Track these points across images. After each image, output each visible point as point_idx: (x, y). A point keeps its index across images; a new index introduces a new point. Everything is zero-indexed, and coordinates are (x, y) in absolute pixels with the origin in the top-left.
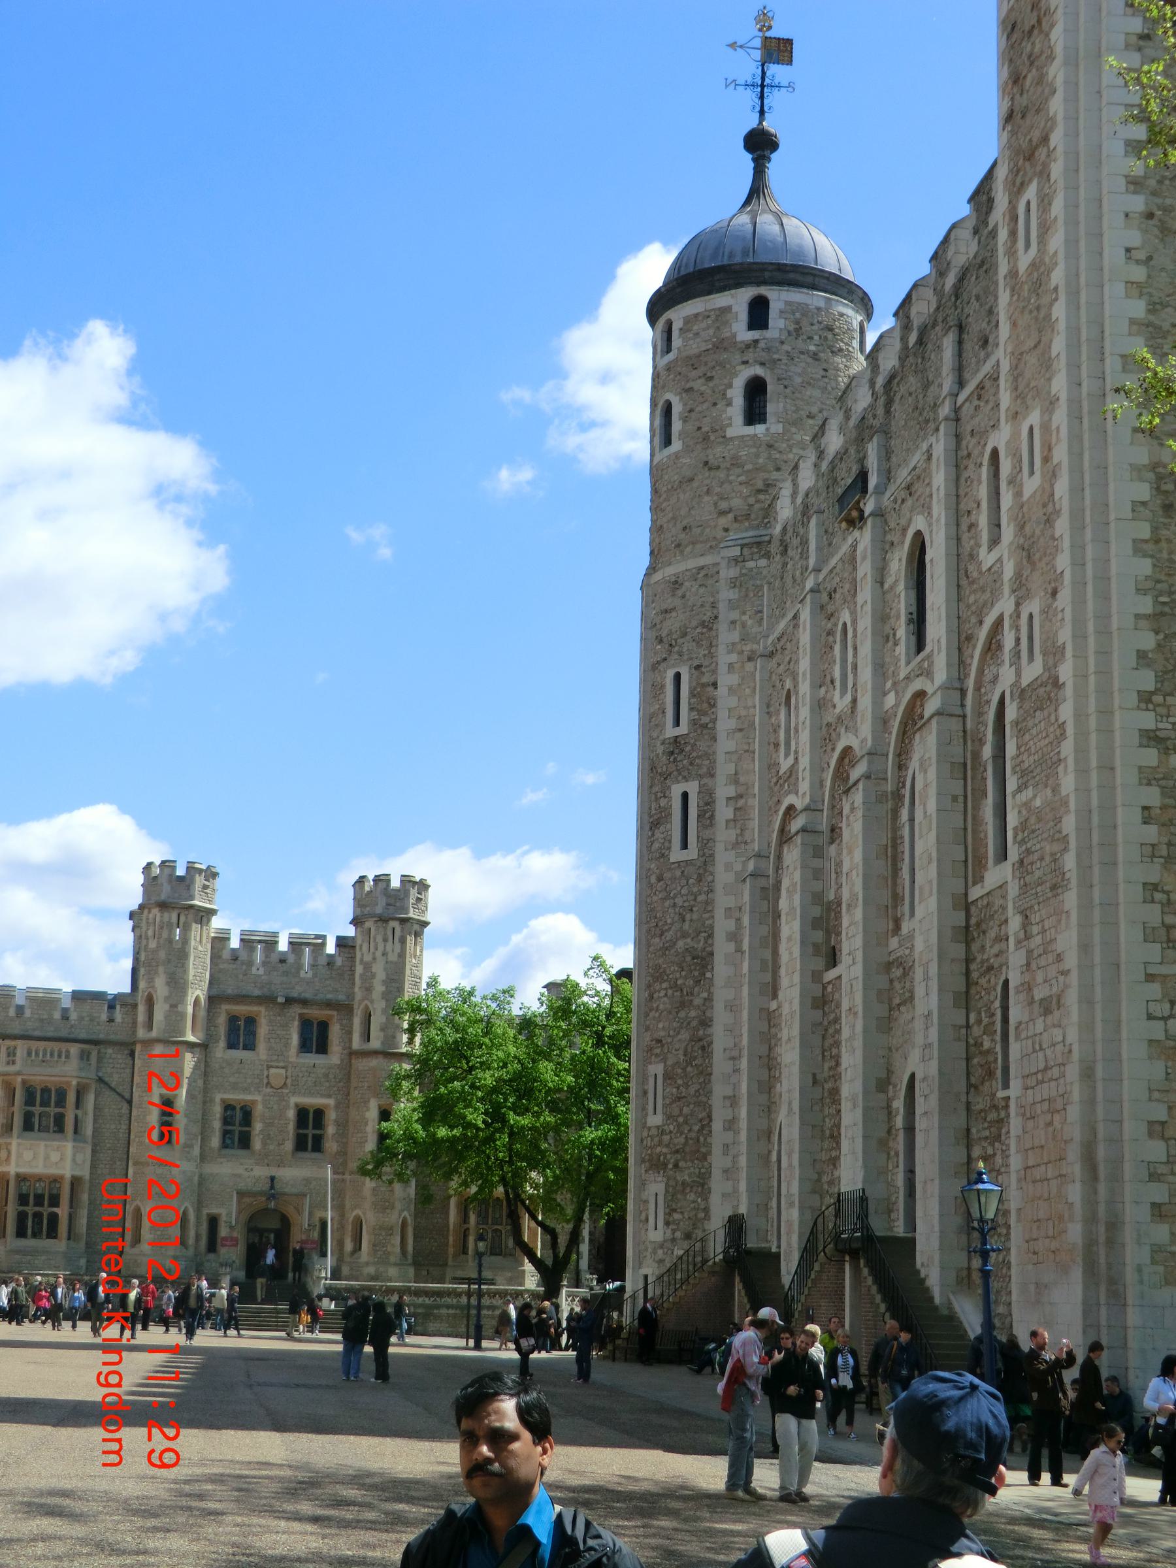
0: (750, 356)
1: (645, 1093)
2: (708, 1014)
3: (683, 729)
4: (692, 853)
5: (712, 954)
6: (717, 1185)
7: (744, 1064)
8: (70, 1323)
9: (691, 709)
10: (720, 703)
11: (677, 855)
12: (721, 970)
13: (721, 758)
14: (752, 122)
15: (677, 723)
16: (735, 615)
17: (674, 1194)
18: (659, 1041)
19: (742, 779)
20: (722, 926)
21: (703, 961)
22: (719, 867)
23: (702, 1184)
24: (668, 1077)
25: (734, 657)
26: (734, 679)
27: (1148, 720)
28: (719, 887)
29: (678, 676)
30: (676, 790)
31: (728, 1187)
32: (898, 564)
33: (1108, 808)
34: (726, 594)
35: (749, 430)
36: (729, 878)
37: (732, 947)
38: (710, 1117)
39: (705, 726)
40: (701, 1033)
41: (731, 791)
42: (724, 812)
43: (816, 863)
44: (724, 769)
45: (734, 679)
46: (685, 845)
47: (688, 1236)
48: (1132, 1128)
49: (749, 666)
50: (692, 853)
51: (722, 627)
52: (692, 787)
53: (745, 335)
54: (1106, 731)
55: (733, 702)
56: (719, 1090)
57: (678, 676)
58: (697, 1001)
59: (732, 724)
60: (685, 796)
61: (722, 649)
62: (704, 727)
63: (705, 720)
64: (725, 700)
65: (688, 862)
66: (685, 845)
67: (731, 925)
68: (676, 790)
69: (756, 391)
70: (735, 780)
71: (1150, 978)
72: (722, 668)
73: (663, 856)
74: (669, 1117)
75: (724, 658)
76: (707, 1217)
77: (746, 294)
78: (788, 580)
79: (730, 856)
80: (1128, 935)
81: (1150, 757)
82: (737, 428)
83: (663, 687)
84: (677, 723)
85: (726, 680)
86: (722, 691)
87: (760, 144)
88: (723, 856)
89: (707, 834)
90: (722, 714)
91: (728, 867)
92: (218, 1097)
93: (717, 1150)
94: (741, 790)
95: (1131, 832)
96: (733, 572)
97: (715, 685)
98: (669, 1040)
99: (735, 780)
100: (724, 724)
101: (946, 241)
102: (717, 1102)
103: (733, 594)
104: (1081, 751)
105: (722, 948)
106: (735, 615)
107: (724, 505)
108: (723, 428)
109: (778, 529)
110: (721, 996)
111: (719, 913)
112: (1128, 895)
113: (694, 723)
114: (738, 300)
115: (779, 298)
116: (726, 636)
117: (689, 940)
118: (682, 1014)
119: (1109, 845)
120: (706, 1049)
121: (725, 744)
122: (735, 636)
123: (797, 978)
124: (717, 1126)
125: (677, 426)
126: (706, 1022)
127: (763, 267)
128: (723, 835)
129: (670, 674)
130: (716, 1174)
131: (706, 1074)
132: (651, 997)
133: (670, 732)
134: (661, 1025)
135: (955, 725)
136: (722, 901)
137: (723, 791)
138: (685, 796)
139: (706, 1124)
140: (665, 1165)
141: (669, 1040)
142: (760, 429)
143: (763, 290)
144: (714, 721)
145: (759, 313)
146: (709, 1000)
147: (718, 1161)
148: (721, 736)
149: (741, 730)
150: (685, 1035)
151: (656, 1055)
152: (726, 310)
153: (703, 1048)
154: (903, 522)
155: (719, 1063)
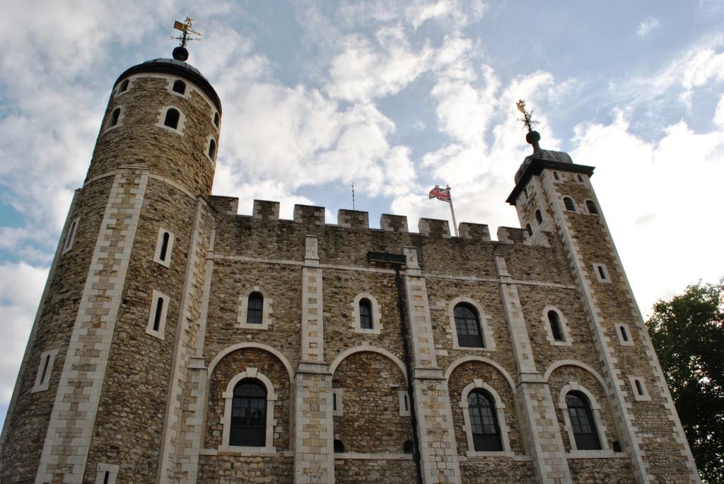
2: (157, 441)
9: (172, 258)
12: (173, 417)
16: (201, 231)
18: (114, 448)
20: (176, 390)
21: (160, 406)
39: (177, 271)
40: (150, 452)
44: (188, 302)
58: (150, 430)
63: (177, 268)
73: (138, 325)
88: (181, 349)
98: (126, 450)
117: (150, 387)
118: (138, 434)
126: (156, 446)
129: (162, 231)
134: (119, 437)
136: (179, 375)
141: (126, 450)
149: (196, 287)
150: (139, 450)
151: (109, 458)
153: (149, 464)
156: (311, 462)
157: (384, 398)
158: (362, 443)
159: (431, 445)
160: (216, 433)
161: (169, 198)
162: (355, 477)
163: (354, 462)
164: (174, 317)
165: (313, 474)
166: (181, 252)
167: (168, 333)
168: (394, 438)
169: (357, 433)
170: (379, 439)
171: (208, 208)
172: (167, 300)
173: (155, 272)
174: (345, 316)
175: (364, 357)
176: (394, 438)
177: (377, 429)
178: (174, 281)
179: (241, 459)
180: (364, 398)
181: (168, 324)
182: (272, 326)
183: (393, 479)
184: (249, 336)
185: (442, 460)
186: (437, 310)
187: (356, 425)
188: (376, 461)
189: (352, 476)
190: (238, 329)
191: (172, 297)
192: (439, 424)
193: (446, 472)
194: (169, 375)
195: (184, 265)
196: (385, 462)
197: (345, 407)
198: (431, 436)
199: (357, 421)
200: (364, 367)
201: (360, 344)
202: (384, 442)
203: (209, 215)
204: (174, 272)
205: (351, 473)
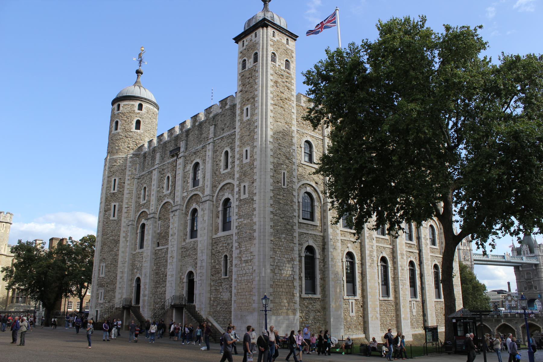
0: (138, 115)
1: (99, 270)
3: (116, 191)
4: (116, 218)
6: (118, 291)
7: (126, 265)
8: (482, 355)
10: (125, 187)
11: (112, 218)
12: (121, 244)
13: (124, 199)
14: (137, 68)
15: (114, 190)
16: (130, 169)
17: (107, 292)
19: (129, 203)
20: (122, 235)
21: (117, 242)
23: (114, 290)
24: (106, 266)
25: (129, 178)
26: (129, 182)
27: (271, 209)
28: (122, 227)
29: (115, 180)
30: (113, 204)
31: (120, 291)
32: (190, 167)
33: (264, 225)
34: (129, 164)
35: (136, 131)
36: (125, 224)
37: (124, 239)
38: (116, 276)
42: (124, 210)
43: (155, 224)
44: (125, 201)
45: (129, 182)
46: (114, 216)
47: (109, 302)
48: (267, 286)
50: (116, 218)
51: (127, 171)
52: (117, 204)
53: (137, 111)
54: (264, 211)
55: (128, 187)
56: (119, 270)
57: (115, 180)
58: (115, 250)
59: (128, 192)
60: (115, 206)
61: (127, 176)
62: (121, 192)
63: (121, 190)
64: (126, 186)
65: (115, 220)
66: (114, 216)
67: (124, 235)
68: (113, 204)
69: (138, 123)
70: (127, 203)
71: (271, 257)
72: (127, 180)
74: (106, 275)
75: (127, 178)
76: (115, 298)
77: (139, 102)
78: (146, 164)
80: (267, 249)
81: (272, 216)
82: (134, 129)
83: (111, 181)
84: (114, 190)
85: (127, 182)
86: (126, 184)
87: (138, 72)
88: (123, 220)
89: (120, 214)
90: (125, 189)
92: (318, 296)
93: (118, 283)
95: (269, 230)
96: (130, 160)
97: (124, 183)
99: (127, 203)
100: (126, 191)
101: (211, 107)
102: (118, 272)
103: (130, 164)
104: (259, 214)
105: (122, 239)
106: (130, 169)
107: (129, 145)
108: (131, 129)
109: (142, 153)
110: (121, 250)
111: (122, 232)
112: (267, 242)
113: (118, 190)
114: (136, 103)
115: (145, 105)
116: (128, 173)
119: (264, 232)
120: (116, 261)
121: (126, 196)
122: (130, 173)
123: (149, 248)
124: (118, 278)
125: (119, 126)
126: (117, 255)
127: (142, 98)
128: (124, 215)
129: (113, 179)
130: (117, 288)
131: (116, 266)
132: (102, 249)
133: (112, 191)
135: (211, 203)
136: (123, 229)
137: (125, 206)
138: (115, 206)
139: (115, 277)
140: (104, 286)
142: (138, 131)
143: (142, 102)
144: (123, 191)
145: (140, 107)
146: (118, 250)
147: (118, 285)
148: (125, 194)
150: (111, 257)
152: (133, 105)
154: (192, 159)
155: (120, 264)
161: (115, 164)
164: (120, 210)
167: (119, 216)
172: (117, 204)
178: (120, 196)
181: (118, 213)
191: (119, 202)
194: (119, 230)
195: (123, 187)
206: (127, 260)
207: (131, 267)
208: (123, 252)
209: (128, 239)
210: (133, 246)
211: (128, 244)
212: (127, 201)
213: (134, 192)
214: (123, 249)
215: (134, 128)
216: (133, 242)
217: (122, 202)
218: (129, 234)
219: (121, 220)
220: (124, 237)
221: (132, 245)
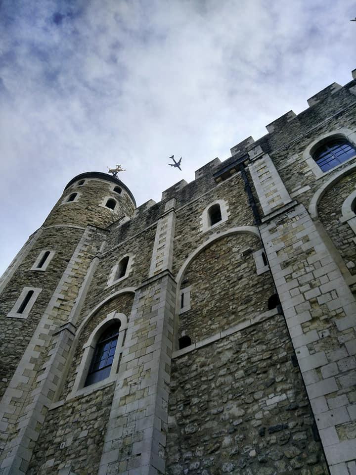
5: (14, 369)
9: (50, 264)
20: (30, 352)
22: (41, 325)
36: (46, 332)
41: (62, 297)
42: (54, 303)
49: (88, 260)
52: (37, 291)
70: (66, 292)
79: (51, 322)
91: (47, 326)
94: (67, 298)
97: (68, 261)
99: (66, 292)
105: (25, 364)
111: (31, 347)
113: (49, 269)
136: (36, 340)
149: (76, 277)
156: (134, 368)
157: (236, 270)
158: (213, 327)
159: (291, 278)
160: (70, 385)
162: (199, 370)
163: (199, 351)
164: (43, 302)
165: (134, 381)
166: (63, 259)
168: (253, 302)
169: (207, 319)
170: (233, 313)
171: (98, 230)
173: (31, 276)
174: (194, 229)
175: (213, 248)
176: (253, 302)
177: (231, 303)
178: (50, 278)
179: (84, 400)
180: (215, 281)
182: (132, 272)
183: (252, 351)
184: (113, 290)
185: (312, 286)
186: (290, 165)
187: (205, 311)
188: (226, 338)
189: (196, 370)
190: (106, 290)
192: (299, 248)
193: (321, 300)
196: (239, 334)
197: (193, 300)
198: (290, 267)
199: (206, 306)
200: (214, 255)
201: (208, 238)
202: (240, 314)
203: (99, 234)
204: (52, 272)
205: (194, 367)
206: (24, 423)
207: (28, 456)
208: (14, 401)
209: (48, 364)
210: (55, 388)
211: (42, 377)
212: (66, 288)
213: (86, 278)
214: (18, 394)
215: (105, 204)
216: (60, 375)
217: (53, 288)
218: (53, 353)
219: (37, 322)
220: (33, 361)
221: (55, 382)
